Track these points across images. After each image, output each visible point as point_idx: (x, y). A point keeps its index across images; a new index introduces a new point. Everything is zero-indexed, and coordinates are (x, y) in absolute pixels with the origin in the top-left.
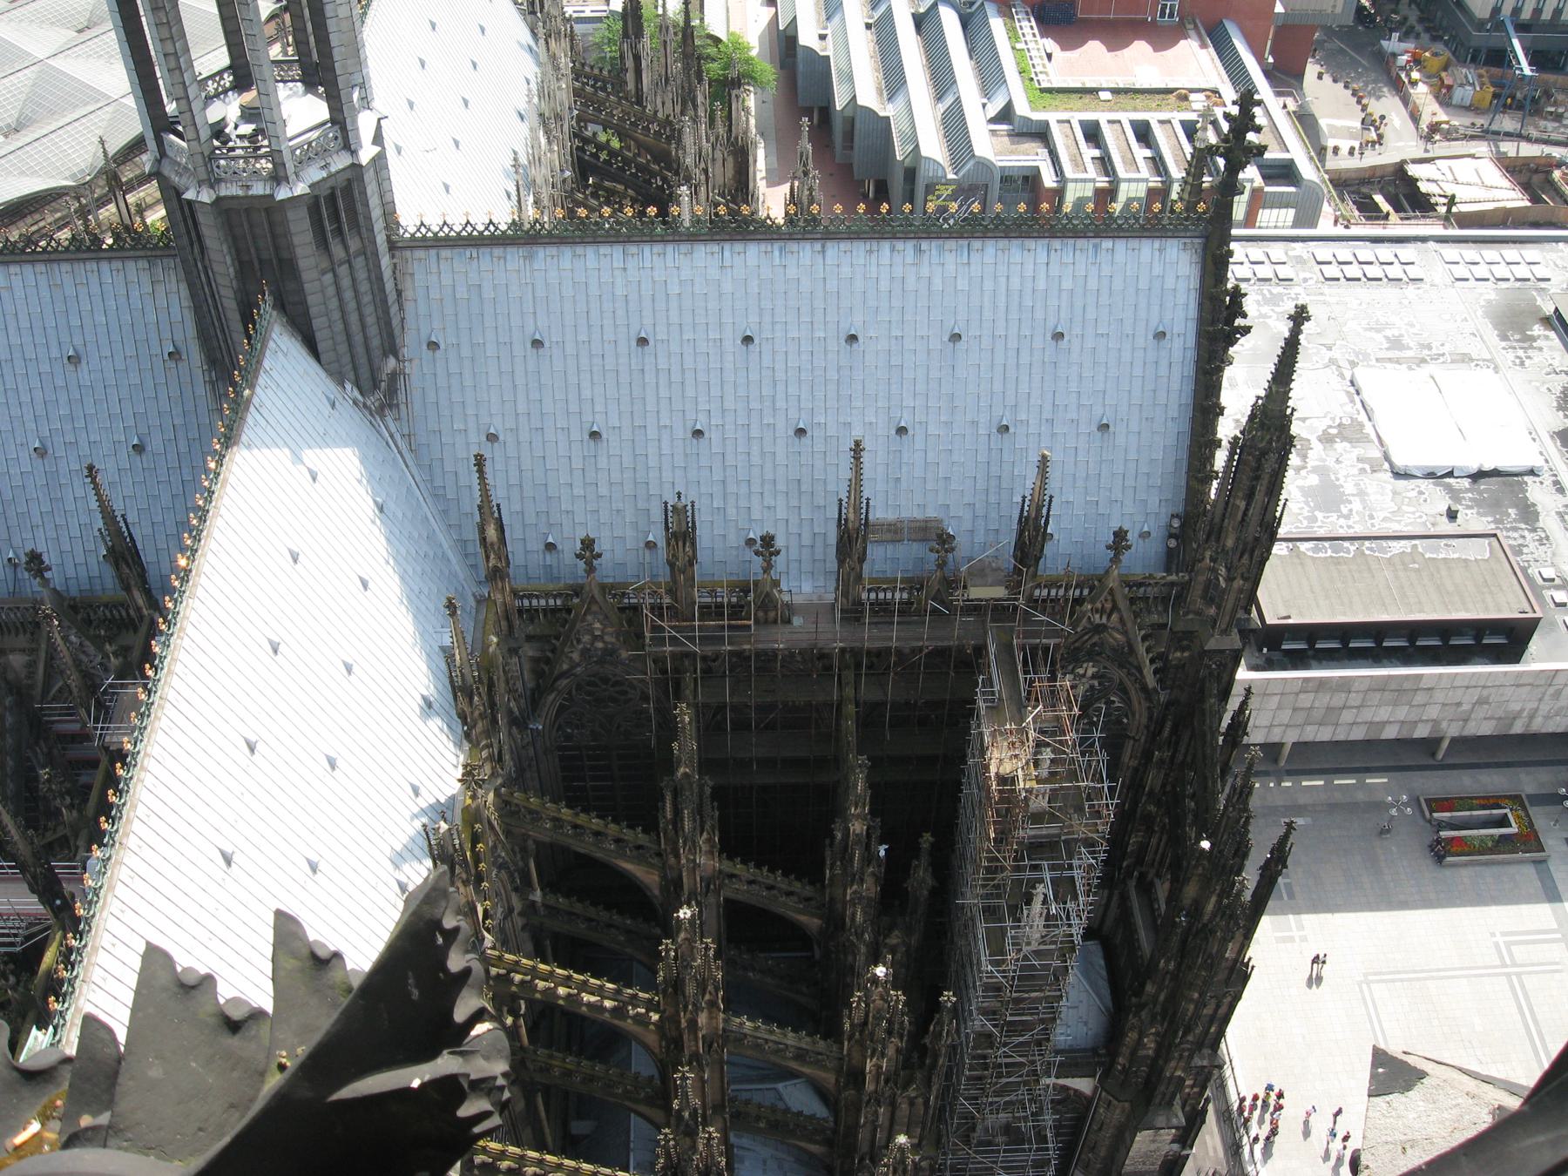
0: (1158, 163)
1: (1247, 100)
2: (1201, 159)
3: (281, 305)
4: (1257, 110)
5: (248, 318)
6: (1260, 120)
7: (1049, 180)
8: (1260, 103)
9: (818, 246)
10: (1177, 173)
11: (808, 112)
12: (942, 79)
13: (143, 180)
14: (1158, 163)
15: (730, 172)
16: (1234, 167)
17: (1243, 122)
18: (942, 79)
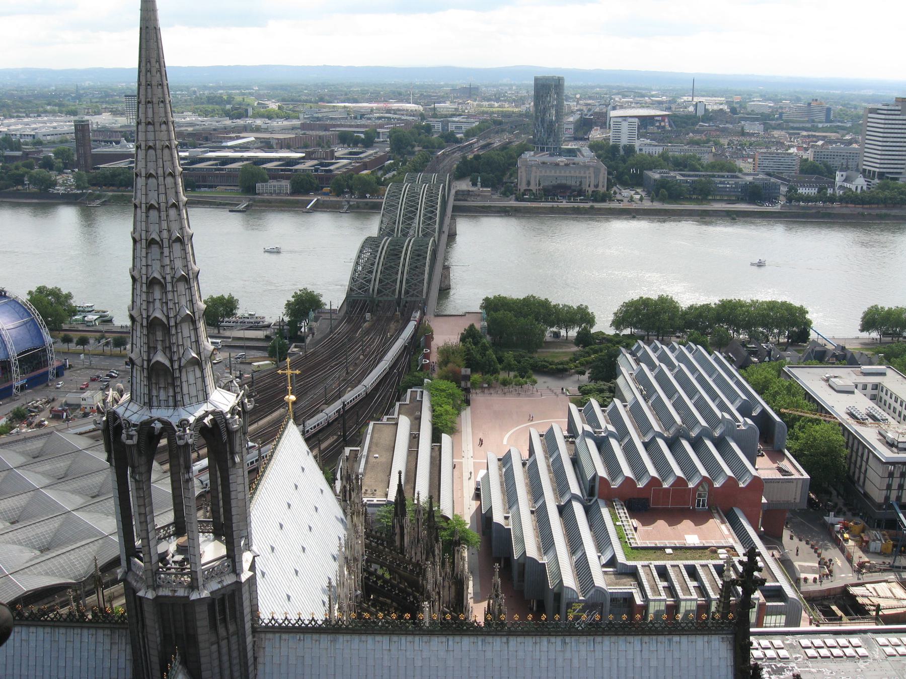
0: (701, 590)
1: (752, 553)
2: (727, 589)
3: (185, 663)
4: (758, 558)
5: (164, 669)
6: (761, 564)
7: (639, 601)
8: (759, 554)
9: (504, 639)
10: (713, 595)
11: (498, 560)
12: (575, 542)
13: (115, 582)
14: (701, 590)
15: (453, 594)
16: (748, 592)
17: (751, 565)
18: (575, 542)
